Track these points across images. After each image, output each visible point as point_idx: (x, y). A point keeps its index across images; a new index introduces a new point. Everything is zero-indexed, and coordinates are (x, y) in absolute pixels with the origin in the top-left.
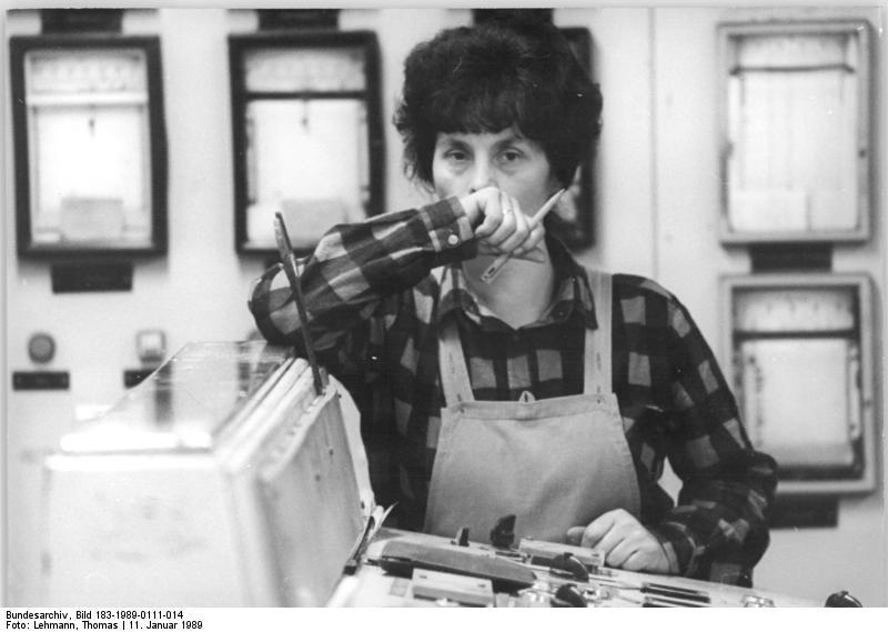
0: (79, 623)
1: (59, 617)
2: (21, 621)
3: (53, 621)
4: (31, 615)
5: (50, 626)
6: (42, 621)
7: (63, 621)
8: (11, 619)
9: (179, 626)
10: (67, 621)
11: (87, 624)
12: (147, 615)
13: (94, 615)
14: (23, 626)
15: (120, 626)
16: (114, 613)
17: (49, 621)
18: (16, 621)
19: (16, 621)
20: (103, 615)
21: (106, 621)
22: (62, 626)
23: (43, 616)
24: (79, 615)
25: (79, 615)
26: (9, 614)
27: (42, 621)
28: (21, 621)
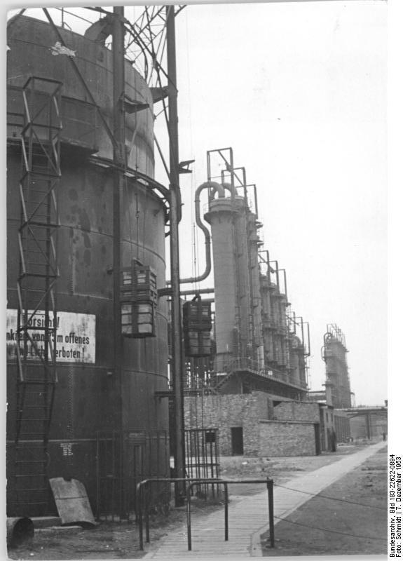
1: (393, 523)
2: (396, 548)
3: (396, 527)
4: (393, 542)
17: (396, 530)
18: (396, 551)
19: (396, 551)
20: (391, 496)
21: (396, 494)
23: (393, 534)
24: (392, 512)
26: (392, 556)
27: (396, 534)
28: (396, 548)
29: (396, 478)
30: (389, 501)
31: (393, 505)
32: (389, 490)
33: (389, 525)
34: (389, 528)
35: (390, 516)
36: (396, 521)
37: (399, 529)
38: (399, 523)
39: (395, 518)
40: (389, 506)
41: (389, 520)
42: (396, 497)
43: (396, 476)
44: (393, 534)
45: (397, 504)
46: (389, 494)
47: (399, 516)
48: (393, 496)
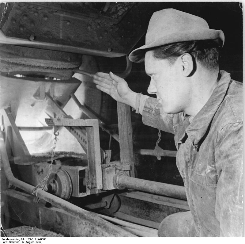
1: (16, 240)
2: (6, 241)
4: (9, 239)
8: (3, 240)
9: (35, 242)
12: (34, 239)
14: (6, 242)
17: (14, 241)
18: (4, 241)
19: (4, 241)
23: (12, 240)
27: (12, 241)
28: (6, 241)
29: (31, 241)
31: (25, 239)
33: (16, 238)
34: (14, 238)
35: (20, 238)
36: (17, 241)
37: (14, 242)
38: (16, 242)
39: (19, 241)
41: (18, 238)
42: (28, 241)
43: (33, 241)
44: (12, 240)
45: (25, 241)
47: (20, 242)
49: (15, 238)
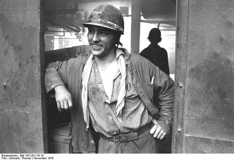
0: (21, 158)
1: (16, 156)
2: (6, 157)
3: (14, 157)
4: (8, 156)
5: (13, 158)
6: (11, 157)
7: (17, 157)
8: (3, 157)
10: (18, 157)
11: (23, 158)
13: (25, 156)
14: (6, 158)
15: (32, 158)
16: (30, 155)
17: (13, 157)
18: (4, 157)
19: (4, 157)
21: (28, 157)
22: (16, 158)
23: (11, 156)
24: (21, 156)
25: (21, 156)
26: (2, 155)
27: (11, 157)
28: (6, 157)
30: (25, 154)
32: (30, 154)
33: (15, 154)
34: (13, 154)
35: (19, 155)
40: (23, 154)
41: (17, 154)
44: (11, 156)
46: (28, 154)
48: (27, 156)
49: (14, 154)
